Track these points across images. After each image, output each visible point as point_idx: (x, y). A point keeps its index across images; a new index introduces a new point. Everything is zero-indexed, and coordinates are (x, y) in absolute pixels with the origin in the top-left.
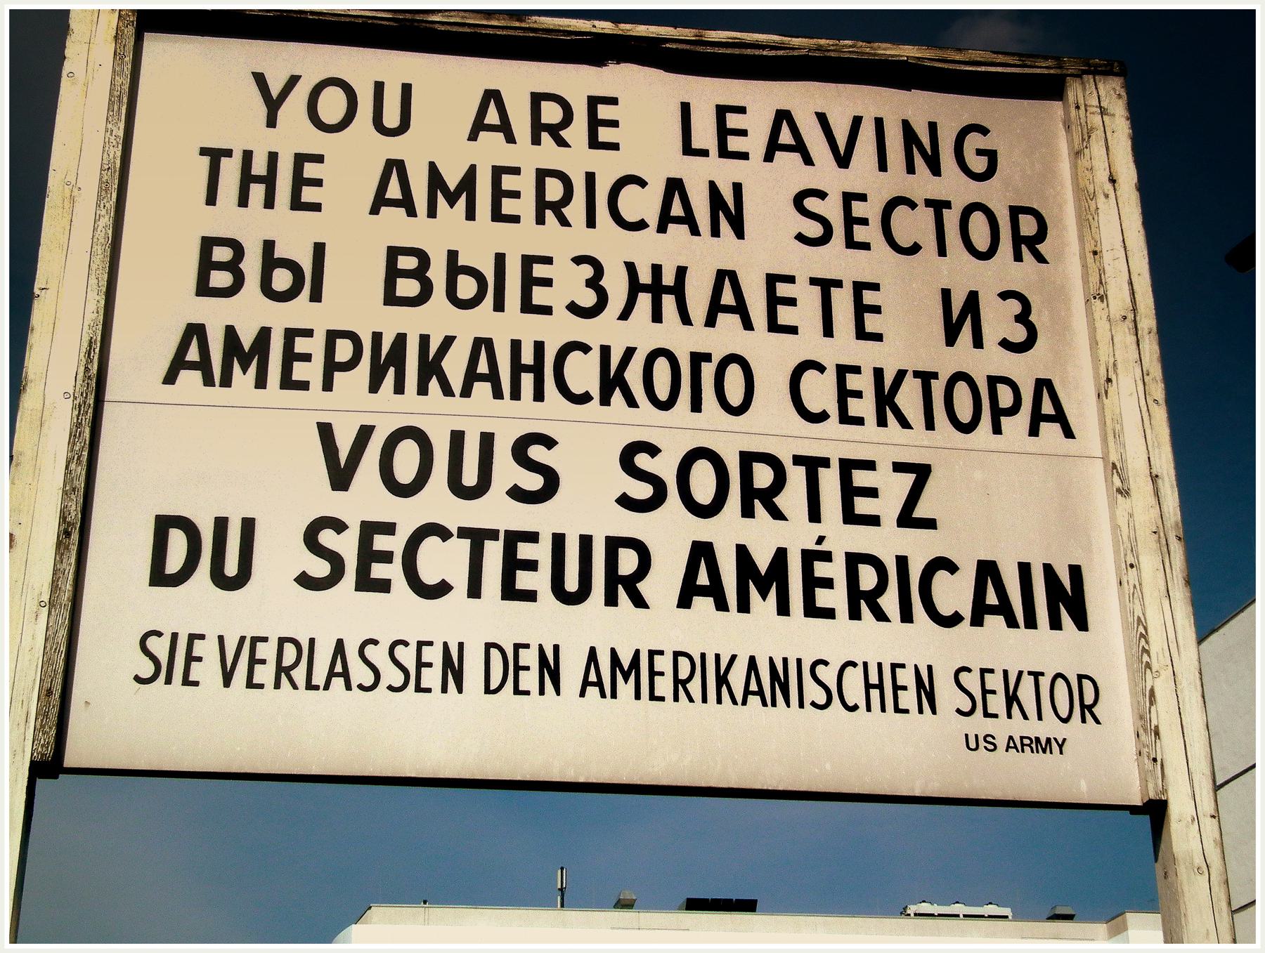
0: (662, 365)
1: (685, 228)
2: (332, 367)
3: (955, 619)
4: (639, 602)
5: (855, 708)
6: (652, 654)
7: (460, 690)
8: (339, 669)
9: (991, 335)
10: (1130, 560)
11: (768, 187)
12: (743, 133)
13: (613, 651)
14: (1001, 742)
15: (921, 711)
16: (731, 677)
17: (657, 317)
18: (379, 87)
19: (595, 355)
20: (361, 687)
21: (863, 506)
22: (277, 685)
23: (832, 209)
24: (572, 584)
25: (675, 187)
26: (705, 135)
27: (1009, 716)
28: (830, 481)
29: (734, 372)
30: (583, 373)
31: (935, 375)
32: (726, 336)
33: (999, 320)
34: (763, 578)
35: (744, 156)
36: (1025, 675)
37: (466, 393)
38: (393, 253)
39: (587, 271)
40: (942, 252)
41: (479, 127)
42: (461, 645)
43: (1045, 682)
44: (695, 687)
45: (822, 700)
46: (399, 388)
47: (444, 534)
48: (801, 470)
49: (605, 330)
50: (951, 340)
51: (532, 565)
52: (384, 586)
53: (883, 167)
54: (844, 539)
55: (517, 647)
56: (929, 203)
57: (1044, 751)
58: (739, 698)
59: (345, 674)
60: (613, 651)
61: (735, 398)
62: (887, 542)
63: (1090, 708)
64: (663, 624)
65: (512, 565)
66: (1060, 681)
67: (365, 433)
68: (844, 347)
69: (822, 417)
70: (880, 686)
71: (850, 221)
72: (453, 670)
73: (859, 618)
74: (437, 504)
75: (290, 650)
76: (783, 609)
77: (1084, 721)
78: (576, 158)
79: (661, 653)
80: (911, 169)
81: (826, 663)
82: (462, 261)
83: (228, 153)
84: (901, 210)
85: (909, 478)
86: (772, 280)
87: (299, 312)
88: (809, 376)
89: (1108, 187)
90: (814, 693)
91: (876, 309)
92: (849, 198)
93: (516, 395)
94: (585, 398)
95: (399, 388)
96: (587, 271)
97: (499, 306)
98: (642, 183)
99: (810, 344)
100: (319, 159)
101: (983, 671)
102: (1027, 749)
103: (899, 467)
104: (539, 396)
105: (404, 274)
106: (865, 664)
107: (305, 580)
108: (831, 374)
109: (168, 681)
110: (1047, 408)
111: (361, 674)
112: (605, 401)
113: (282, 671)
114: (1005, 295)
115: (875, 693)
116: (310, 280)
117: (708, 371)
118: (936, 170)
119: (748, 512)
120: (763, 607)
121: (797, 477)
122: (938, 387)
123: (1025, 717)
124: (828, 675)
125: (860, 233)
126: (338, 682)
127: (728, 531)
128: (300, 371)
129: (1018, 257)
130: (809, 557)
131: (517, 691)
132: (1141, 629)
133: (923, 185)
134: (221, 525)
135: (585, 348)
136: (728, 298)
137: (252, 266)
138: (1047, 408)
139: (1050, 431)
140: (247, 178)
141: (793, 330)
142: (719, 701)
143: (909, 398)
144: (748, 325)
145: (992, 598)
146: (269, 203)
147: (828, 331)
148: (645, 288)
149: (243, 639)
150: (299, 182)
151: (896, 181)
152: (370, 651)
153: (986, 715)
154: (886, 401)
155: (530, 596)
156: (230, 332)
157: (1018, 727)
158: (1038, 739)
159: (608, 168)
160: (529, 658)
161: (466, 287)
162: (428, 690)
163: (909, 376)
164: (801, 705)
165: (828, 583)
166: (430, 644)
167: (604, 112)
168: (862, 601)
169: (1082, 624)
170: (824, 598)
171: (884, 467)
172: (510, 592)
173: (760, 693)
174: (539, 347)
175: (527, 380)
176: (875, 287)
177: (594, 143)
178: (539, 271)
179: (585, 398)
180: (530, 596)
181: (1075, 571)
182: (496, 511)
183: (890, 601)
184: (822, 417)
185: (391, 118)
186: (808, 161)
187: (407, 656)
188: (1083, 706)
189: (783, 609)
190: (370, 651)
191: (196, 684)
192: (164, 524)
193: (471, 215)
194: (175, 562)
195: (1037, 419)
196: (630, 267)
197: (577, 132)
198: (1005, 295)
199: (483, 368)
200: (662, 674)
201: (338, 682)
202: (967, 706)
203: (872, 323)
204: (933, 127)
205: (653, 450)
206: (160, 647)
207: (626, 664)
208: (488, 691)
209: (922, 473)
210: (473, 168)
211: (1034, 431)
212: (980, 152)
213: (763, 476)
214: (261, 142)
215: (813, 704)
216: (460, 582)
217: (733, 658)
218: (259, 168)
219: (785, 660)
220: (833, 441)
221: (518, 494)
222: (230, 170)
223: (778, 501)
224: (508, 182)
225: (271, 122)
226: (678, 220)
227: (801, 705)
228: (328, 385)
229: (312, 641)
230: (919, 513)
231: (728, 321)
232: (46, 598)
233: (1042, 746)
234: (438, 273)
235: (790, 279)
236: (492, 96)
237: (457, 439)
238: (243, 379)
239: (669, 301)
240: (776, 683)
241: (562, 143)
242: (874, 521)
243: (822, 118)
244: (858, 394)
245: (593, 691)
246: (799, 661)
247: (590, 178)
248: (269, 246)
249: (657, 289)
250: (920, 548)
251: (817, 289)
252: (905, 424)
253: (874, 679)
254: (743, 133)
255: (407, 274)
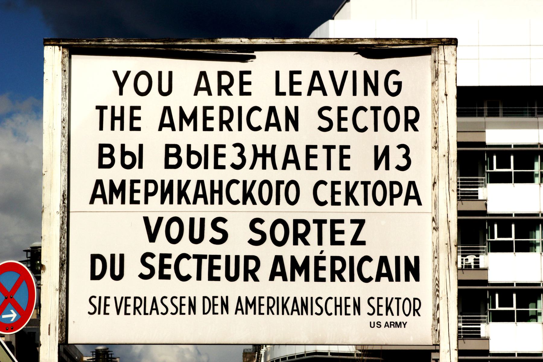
0: (266, 187)
1: (275, 128)
2: (147, 195)
3: (370, 279)
4: (256, 279)
5: (331, 314)
6: (260, 298)
7: (195, 313)
8: (154, 307)
9: (392, 165)
10: (436, 255)
11: (308, 106)
12: (299, 83)
13: (247, 298)
14: (383, 324)
15: (354, 314)
16: (287, 305)
17: (264, 167)
18: (160, 73)
19: (241, 184)
20: (162, 313)
21: (338, 237)
22: (134, 314)
23: (333, 115)
24: (232, 274)
25: (272, 110)
26: (284, 86)
27: (387, 315)
28: (326, 228)
29: (292, 187)
30: (236, 192)
31: (369, 183)
32: (290, 173)
33: (396, 157)
34: (300, 268)
35: (299, 94)
36: (394, 299)
37: (195, 202)
38: (168, 146)
39: (238, 149)
40: (376, 130)
41: (198, 89)
42: (195, 298)
43: (401, 302)
44: (275, 309)
45: (319, 311)
46: (171, 202)
47: (188, 257)
48: (316, 225)
49: (245, 174)
50: (377, 167)
51: (218, 268)
52: (168, 277)
53: (355, 94)
54: (330, 251)
55: (214, 297)
56: (372, 108)
57: (398, 327)
58: (290, 313)
59: (157, 309)
60: (247, 298)
61: (292, 198)
62: (346, 251)
63: (417, 310)
64: (265, 287)
65: (212, 267)
66: (407, 301)
67: (160, 220)
68: (336, 174)
69: (325, 203)
70: (340, 306)
71: (341, 119)
72: (192, 306)
73: (334, 281)
74: (185, 246)
75: (138, 301)
76: (307, 279)
77: (414, 315)
78: (234, 101)
79: (263, 297)
80: (366, 94)
81: (321, 298)
82: (192, 149)
83: (106, 108)
84: (361, 112)
85: (356, 226)
86: (308, 147)
87: (135, 173)
88: (321, 186)
89: (445, 97)
90: (317, 309)
91: (348, 157)
92: (340, 109)
93: (212, 203)
94: (237, 202)
95: (171, 202)
96: (238, 149)
97: (206, 167)
98: (259, 109)
99: (322, 174)
100: (139, 108)
101: (379, 298)
102: (392, 326)
103: (353, 221)
104: (221, 202)
105: (172, 155)
106: (336, 298)
107: (142, 276)
108: (329, 185)
109: (99, 313)
110: (412, 194)
111: (162, 309)
112: (244, 203)
113: (136, 308)
114: (399, 147)
115: (338, 308)
116: (137, 160)
117: (283, 187)
118: (376, 93)
119: (295, 243)
120: (300, 278)
121: (314, 227)
122: (370, 188)
123: (393, 315)
124: (322, 303)
125: (344, 124)
126: (154, 312)
127: (288, 251)
128: (137, 197)
129: (406, 129)
130: (317, 259)
131: (214, 313)
132: (437, 282)
133: (371, 100)
134: (113, 256)
135: (237, 182)
136: (291, 157)
137: (117, 155)
138: (412, 193)
139: (413, 202)
140: (114, 118)
141: (315, 168)
142: (283, 314)
143: (359, 193)
144: (298, 168)
145: (384, 271)
146: (122, 129)
147: (329, 168)
148: (260, 155)
149: (122, 298)
150: (133, 118)
151: (361, 100)
152: (164, 300)
153: (378, 314)
154: (349, 194)
155: (218, 279)
156: (111, 182)
157: (390, 318)
158: (396, 323)
159: (247, 103)
160: (218, 301)
161: (194, 159)
162: (184, 314)
163: (360, 183)
164: (312, 314)
165: (324, 268)
166: (184, 297)
167: (246, 78)
168: (336, 274)
169: (417, 279)
170: (322, 274)
171: (347, 221)
172: (211, 278)
173: (297, 310)
174: (221, 182)
175: (216, 196)
176: (348, 147)
177: (242, 93)
178: (221, 151)
179: (237, 202)
180: (218, 279)
181: (417, 259)
182: (206, 248)
183: (346, 274)
184: (325, 203)
185: (165, 89)
186: (325, 94)
187: (177, 302)
188: (414, 310)
189: (307, 279)
190: (164, 300)
191: (108, 314)
192: (94, 257)
193: (195, 129)
194: (98, 272)
195: (408, 197)
196: (255, 147)
197: (235, 89)
198: (399, 147)
199: (200, 192)
200: (263, 305)
201: (154, 312)
202: (371, 311)
203: (346, 163)
204: (376, 73)
205: (261, 221)
206: (95, 301)
207: (251, 301)
208: (204, 313)
209: (361, 223)
210: (196, 108)
211: (406, 203)
212: (395, 83)
213: (302, 228)
214: (118, 102)
215: (316, 313)
216: (194, 275)
217: (288, 298)
218: (118, 114)
219: (307, 298)
220: (329, 213)
221: (213, 241)
222: (107, 114)
223: (307, 238)
224: (209, 113)
225: (121, 93)
226: (273, 125)
227: (312, 314)
228: (146, 202)
229: (145, 298)
230: (359, 239)
231: (291, 167)
232: (58, 287)
233: (397, 325)
234: (183, 154)
235: (315, 147)
236: (203, 74)
237: (192, 220)
238: (117, 201)
239: (269, 160)
240: (303, 306)
241: (229, 94)
242: (342, 243)
243: (331, 73)
244: (339, 193)
245: (239, 312)
246: (312, 298)
247: (240, 108)
248: (123, 146)
249: (264, 155)
250: (358, 252)
251: (326, 150)
252: (356, 203)
253: (338, 303)
254: (299, 83)
255: (173, 155)
